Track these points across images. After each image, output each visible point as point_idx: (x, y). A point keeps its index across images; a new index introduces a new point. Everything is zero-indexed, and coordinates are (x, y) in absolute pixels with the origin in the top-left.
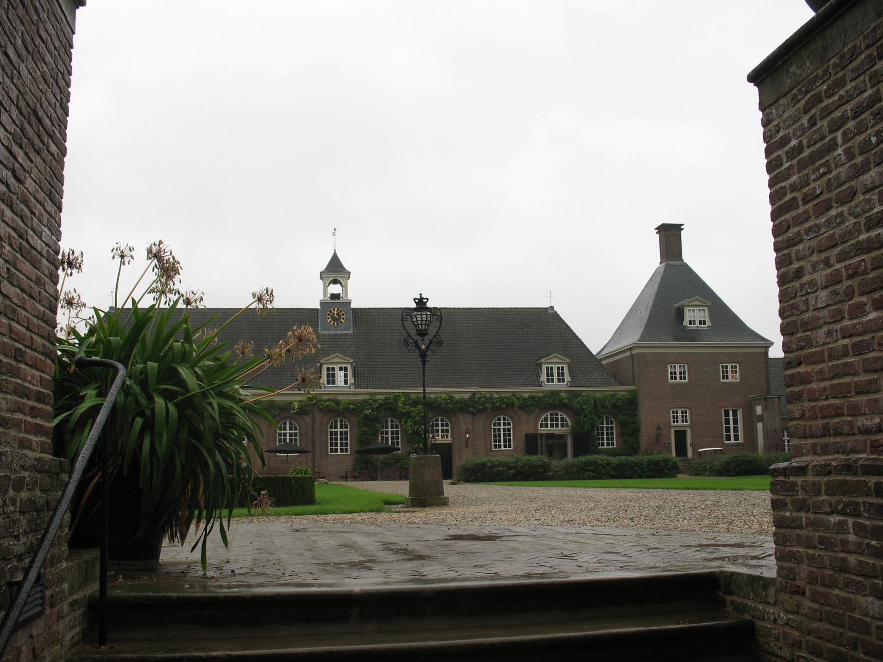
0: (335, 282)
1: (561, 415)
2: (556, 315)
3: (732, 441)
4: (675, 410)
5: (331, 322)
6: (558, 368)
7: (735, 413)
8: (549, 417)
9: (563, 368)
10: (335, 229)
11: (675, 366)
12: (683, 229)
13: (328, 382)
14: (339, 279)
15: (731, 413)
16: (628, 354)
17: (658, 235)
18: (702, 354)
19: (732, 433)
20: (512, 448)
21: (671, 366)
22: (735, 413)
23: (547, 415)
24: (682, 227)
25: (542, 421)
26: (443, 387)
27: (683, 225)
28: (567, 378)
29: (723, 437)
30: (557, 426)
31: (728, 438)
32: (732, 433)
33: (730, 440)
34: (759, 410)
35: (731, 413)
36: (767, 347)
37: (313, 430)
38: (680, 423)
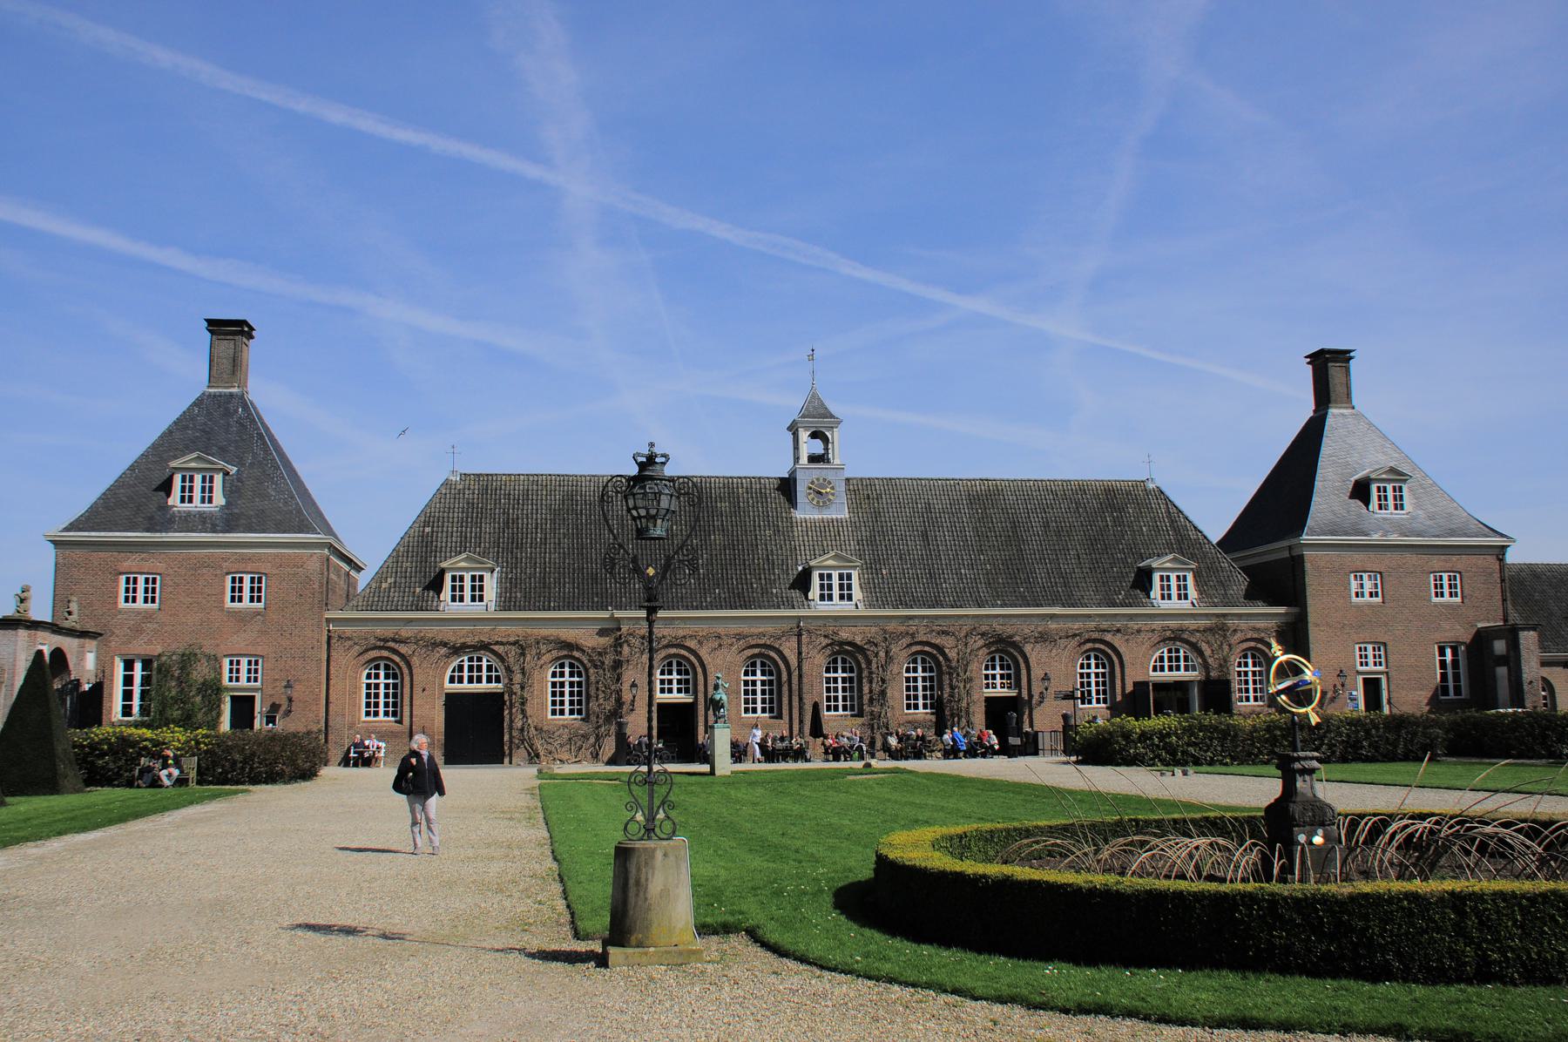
0: (814, 435)
3: (1452, 696)
4: (1362, 646)
5: (813, 499)
8: (1166, 655)
10: (813, 350)
11: (1361, 576)
12: (1351, 358)
13: (822, 597)
16: (1286, 554)
17: (1310, 366)
19: (1451, 684)
21: (1356, 576)
23: (1163, 653)
24: (1352, 354)
26: (1004, 605)
27: (1350, 351)
28: (1192, 593)
30: (1178, 668)
32: (1451, 684)
33: (1448, 695)
34: (1500, 646)
36: (1504, 548)
37: (800, 676)
38: (1371, 667)
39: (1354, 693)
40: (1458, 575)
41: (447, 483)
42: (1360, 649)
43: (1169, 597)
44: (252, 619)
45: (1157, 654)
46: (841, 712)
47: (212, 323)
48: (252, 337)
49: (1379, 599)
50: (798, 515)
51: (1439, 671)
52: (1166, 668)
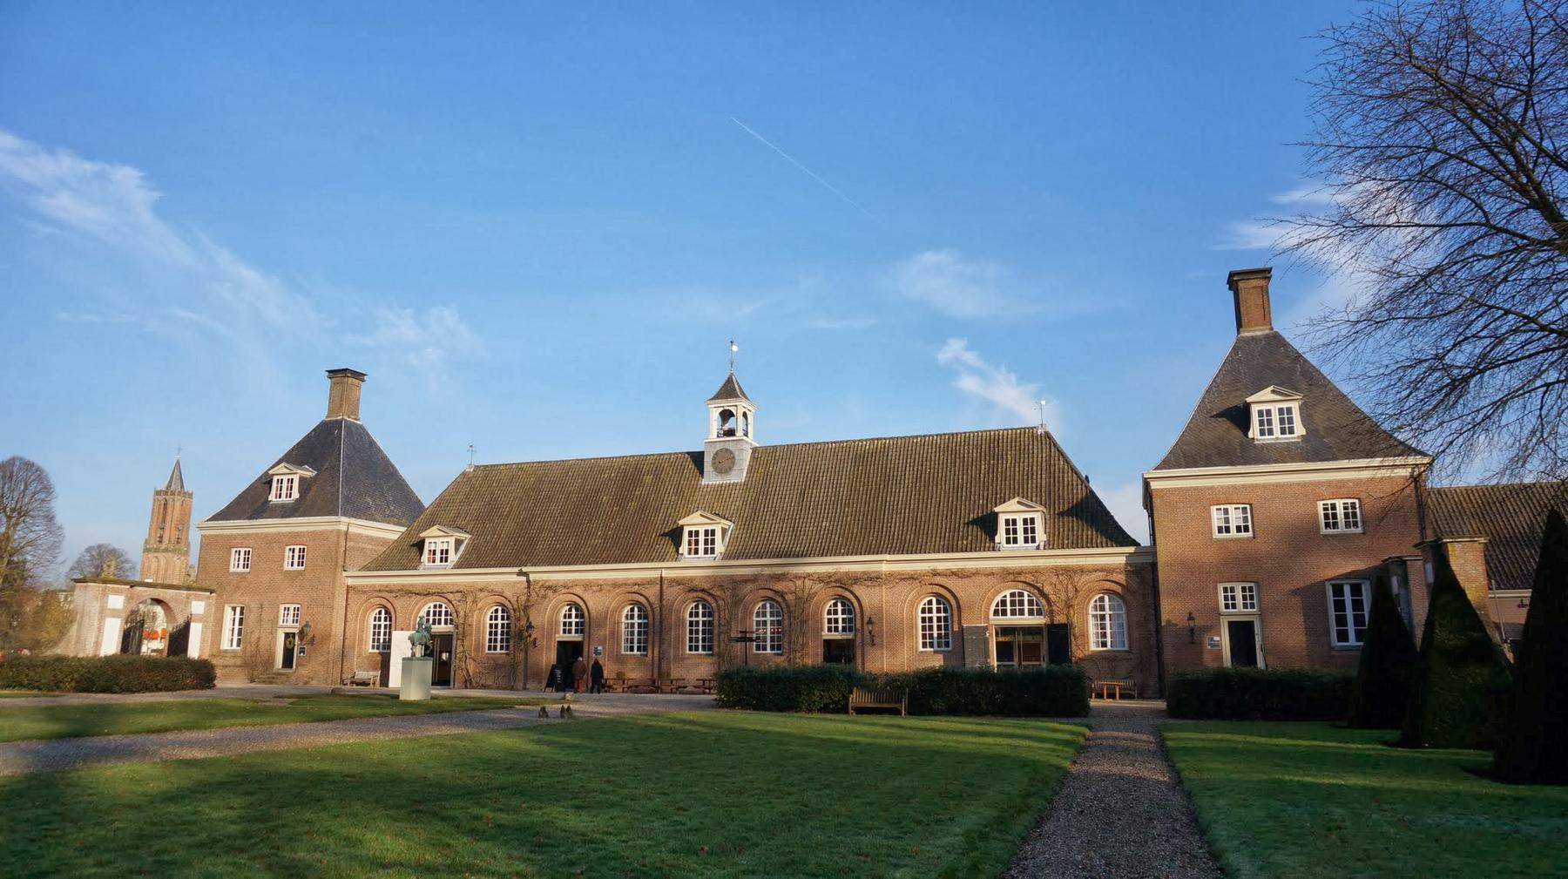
1: (1029, 596)
2: (1048, 435)
6: (1025, 521)
7: (1356, 590)
8: (1008, 599)
9: (1032, 521)
14: (730, 408)
15: (1347, 590)
18: (1278, 486)
20: (950, 649)
22: (1356, 590)
23: (1005, 596)
25: (997, 605)
29: (1328, 633)
30: (1022, 612)
31: (1343, 636)
33: (1347, 640)
35: (1347, 590)
39: (1216, 638)
40: (1248, 506)
41: (464, 474)
42: (1225, 590)
43: (1015, 541)
44: (297, 577)
45: (999, 598)
46: (700, 651)
47: (329, 371)
48: (363, 381)
49: (1250, 534)
50: (704, 482)
51: (1332, 613)
52: (1026, 612)
